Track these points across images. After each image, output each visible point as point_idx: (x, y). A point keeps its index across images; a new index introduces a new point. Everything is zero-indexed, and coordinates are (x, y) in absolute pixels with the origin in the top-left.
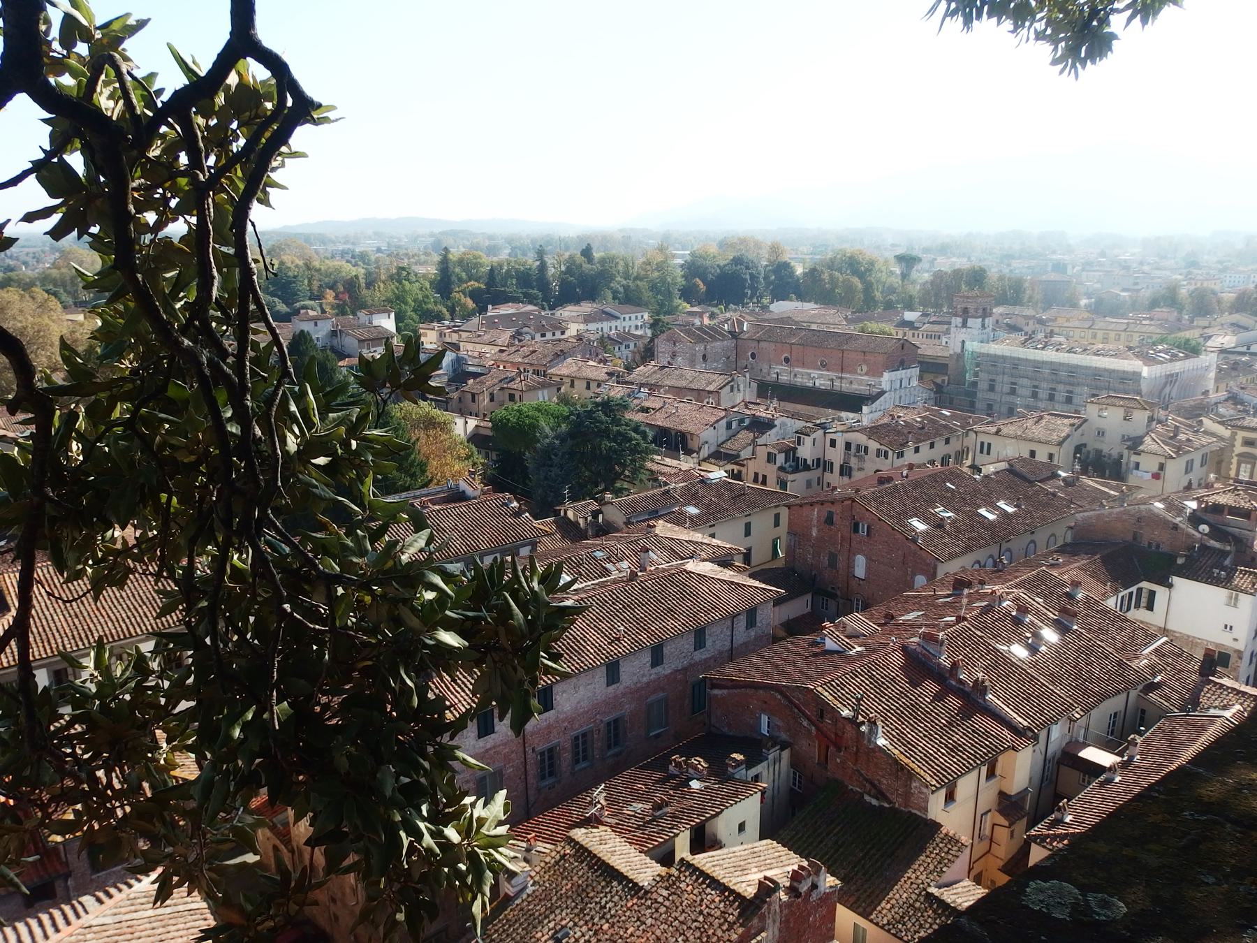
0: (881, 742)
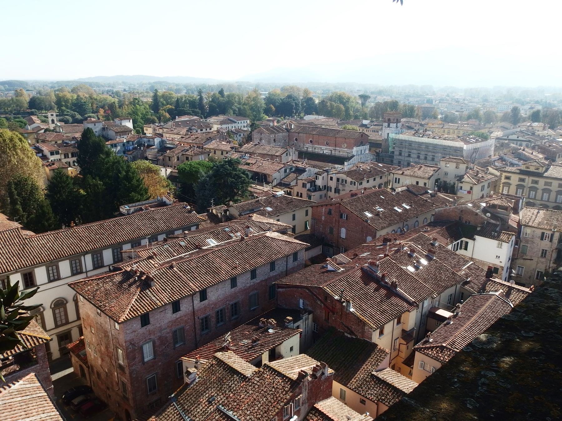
0: (352, 310)
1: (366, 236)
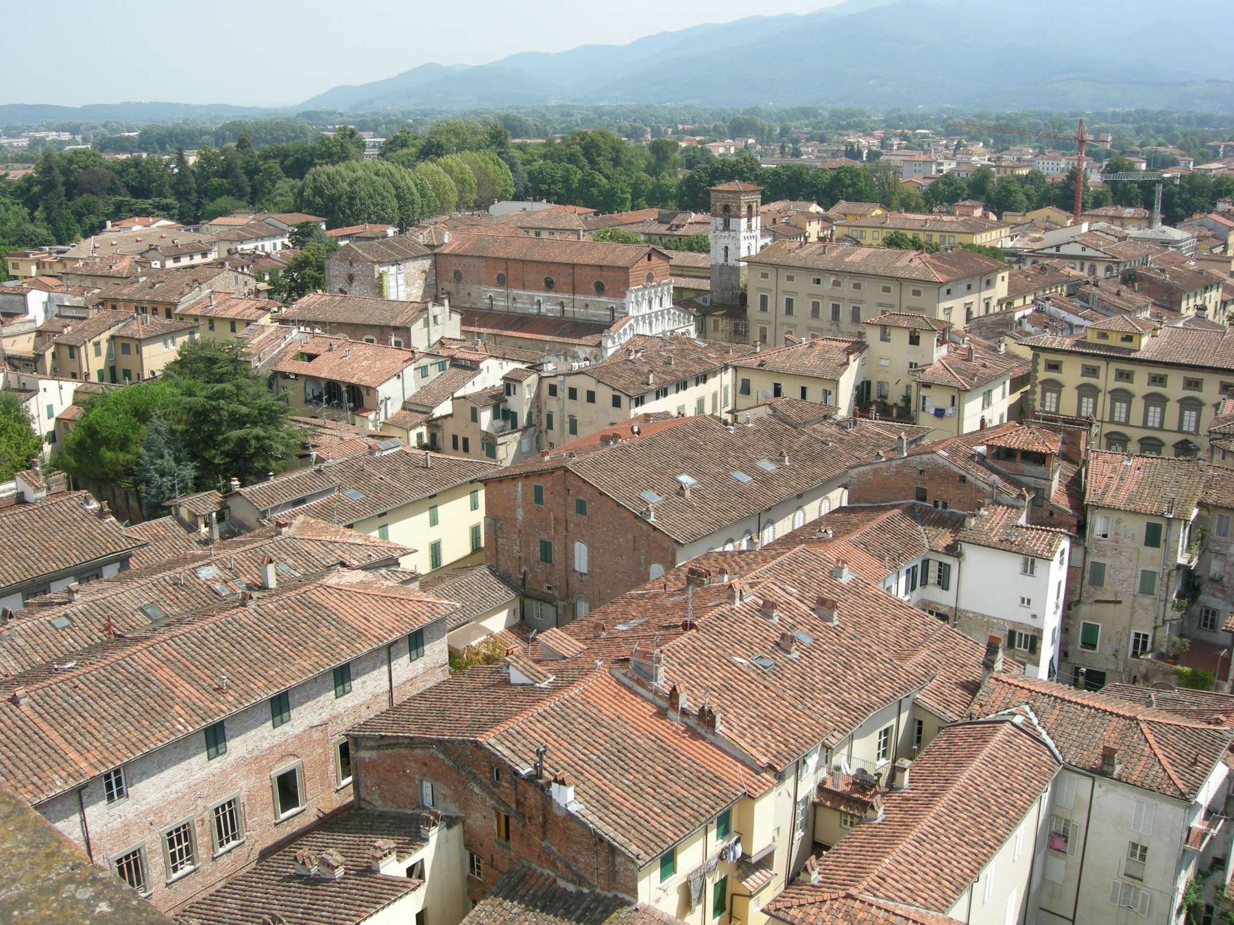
1: (648, 563)
